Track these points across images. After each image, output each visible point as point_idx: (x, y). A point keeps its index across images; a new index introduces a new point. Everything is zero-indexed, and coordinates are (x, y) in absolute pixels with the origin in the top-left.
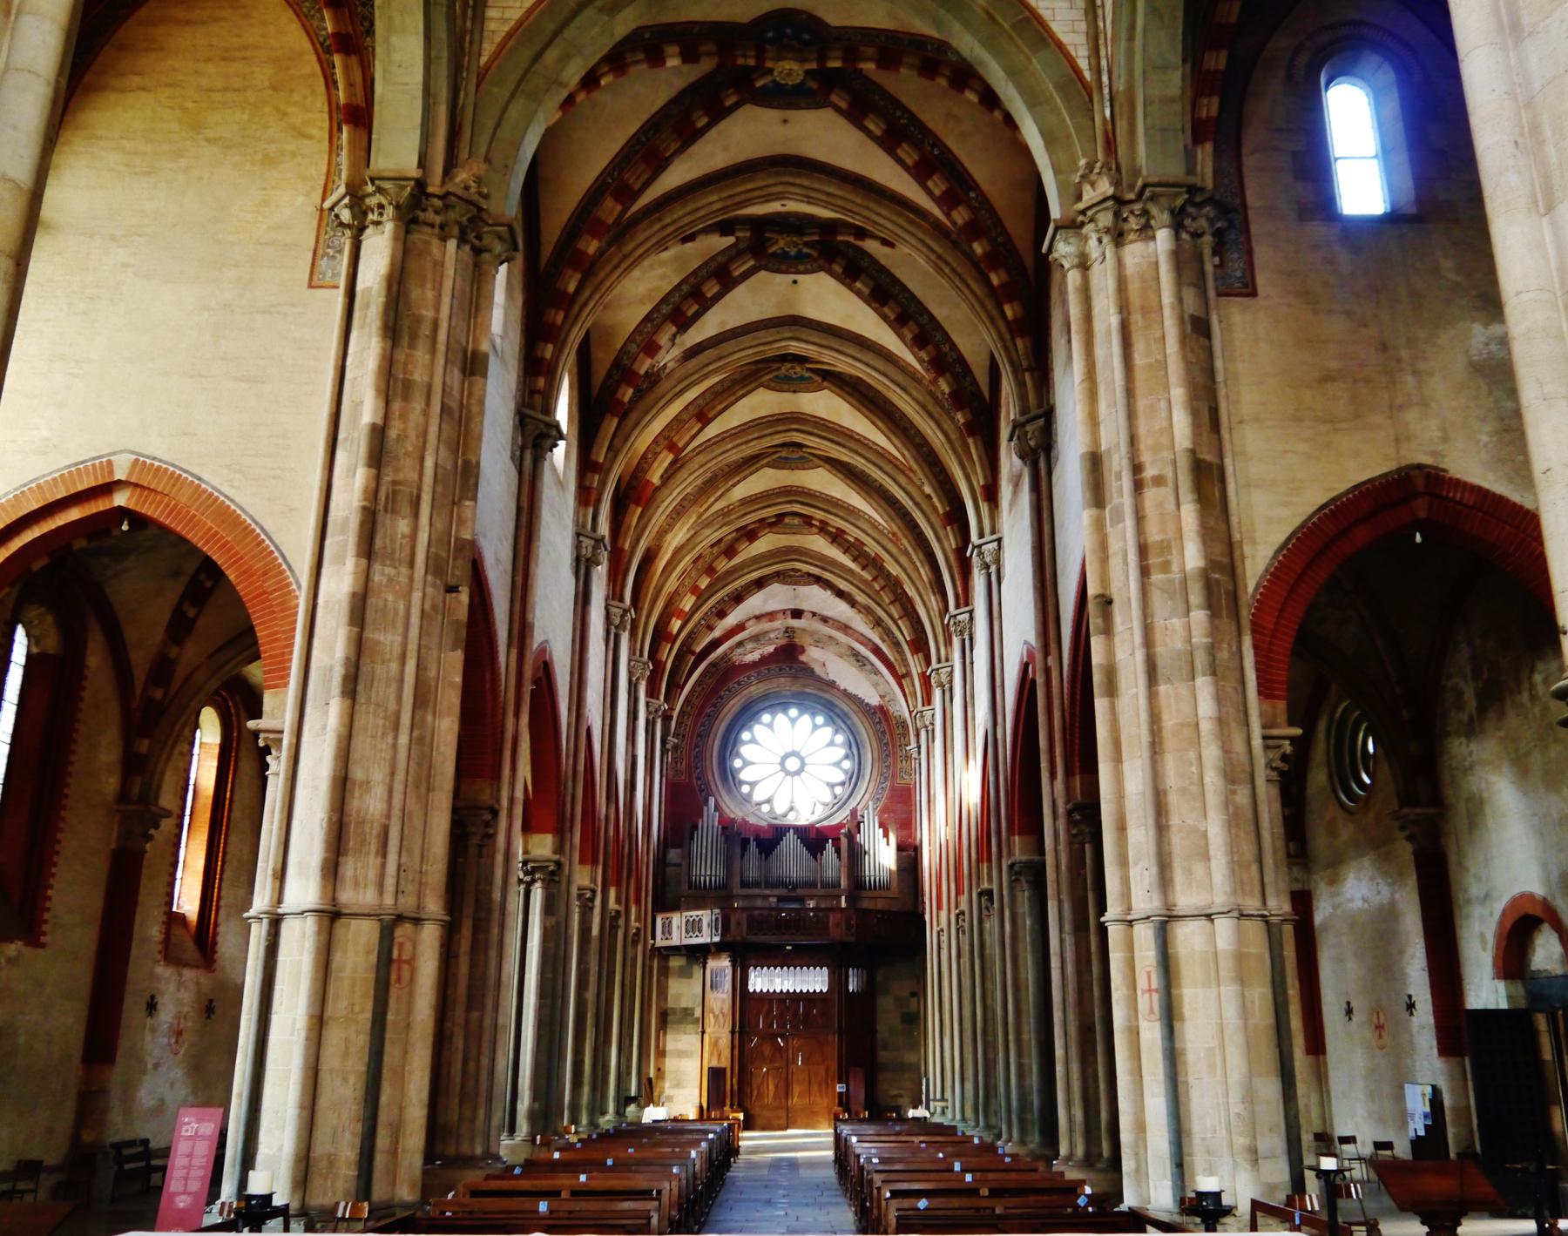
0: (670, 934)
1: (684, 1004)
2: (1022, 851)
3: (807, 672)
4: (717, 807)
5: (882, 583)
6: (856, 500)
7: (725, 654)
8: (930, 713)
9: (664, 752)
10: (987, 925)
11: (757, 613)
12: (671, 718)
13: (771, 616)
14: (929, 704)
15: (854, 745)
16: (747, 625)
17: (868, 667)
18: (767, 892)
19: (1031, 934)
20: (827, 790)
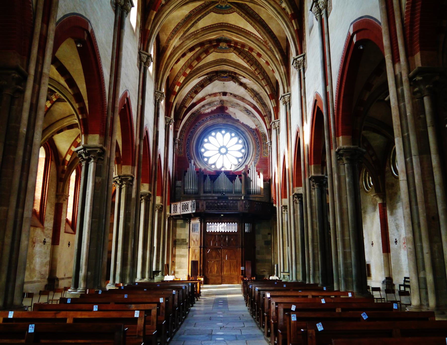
1: (182, 238)
2: (343, 144)
3: (229, 117)
4: (194, 164)
5: (259, 71)
6: (250, 28)
7: (198, 110)
8: (278, 122)
9: (174, 144)
10: (313, 193)
11: (210, 93)
12: (177, 131)
13: (215, 94)
15: (246, 144)
16: (206, 98)
17: (251, 115)
18: (214, 195)
19: (349, 186)
20: (236, 160)
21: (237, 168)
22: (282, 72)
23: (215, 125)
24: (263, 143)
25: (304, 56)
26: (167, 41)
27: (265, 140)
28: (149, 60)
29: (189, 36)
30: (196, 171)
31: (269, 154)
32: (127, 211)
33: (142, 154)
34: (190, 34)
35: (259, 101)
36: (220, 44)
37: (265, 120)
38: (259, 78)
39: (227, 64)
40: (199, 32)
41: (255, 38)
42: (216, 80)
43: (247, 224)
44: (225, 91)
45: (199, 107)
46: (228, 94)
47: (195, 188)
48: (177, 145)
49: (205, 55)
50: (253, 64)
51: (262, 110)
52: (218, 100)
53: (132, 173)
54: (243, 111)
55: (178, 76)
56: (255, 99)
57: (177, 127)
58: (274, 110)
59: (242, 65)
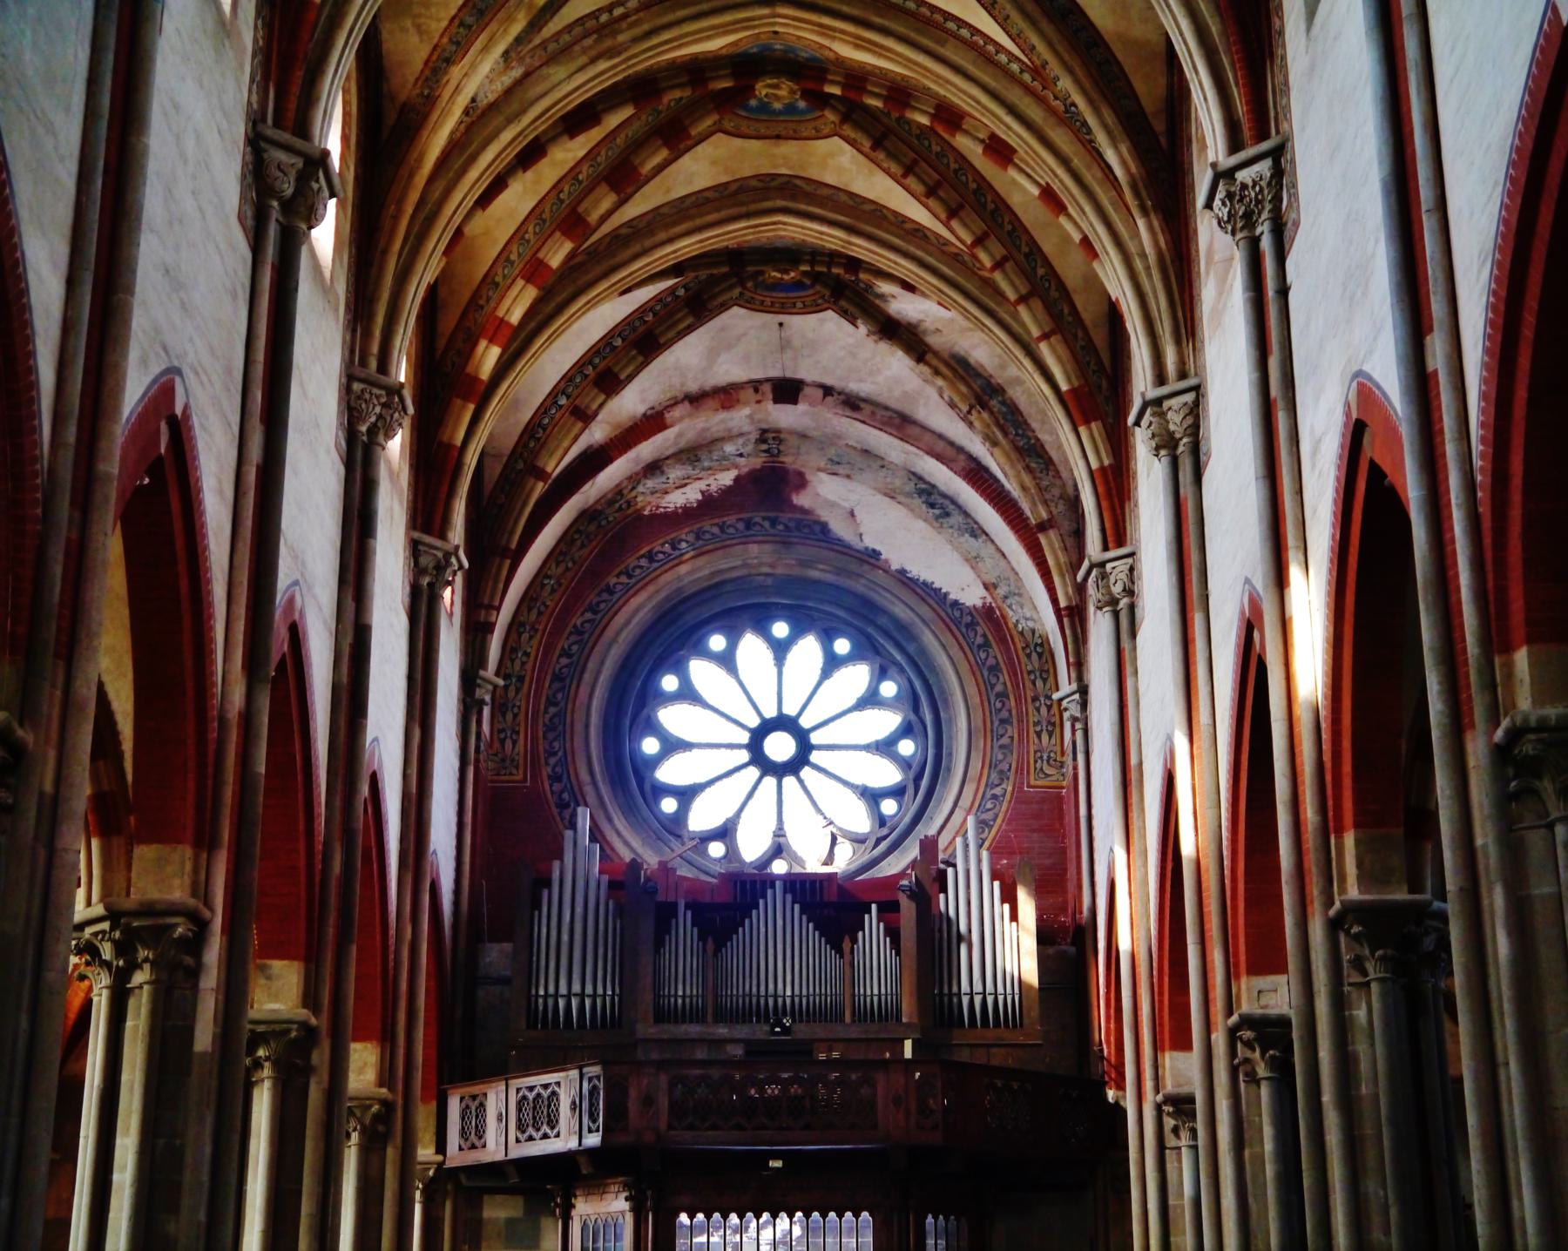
0: (480, 1134)
2: (1539, 699)
5: (1000, 251)
7: (618, 494)
8: (1122, 566)
10: (1361, 1014)
11: (693, 387)
12: (490, 628)
13: (726, 395)
14: (1121, 542)
16: (668, 416)
17: (957, 519)
18: (722, 1031)
21: (866, 858)
22: (1143, 255)
23: (729, 587)
24: (1030, 694)
25: (1279, 154)
26: (427, 73)
27: (1045, 681)
28: (315, 186)
29: (566, 38)
30: (605, 878)
31: (1075, 768)
32: (161, 1142)
33: (262, 769)
34: (569, 28)
35: (1006, 434)
36: (759, 86)
37: (1041, 550)
38: (1002, 295)
39: (803, 207)
40: (625, 16)
41: (972, 46)
42: (735, 309)
43: (936, 1218)
44: (789, 374)
45: (629, 473)
46: (807, 390)
47: (600, 991)
48: (486, 711)
49: (664, 154)
50: (961, 207)
51: (1024, 488)
52: (746, 428)
53: (194, 894)
55: (497, 285)
56: (977, 424)
57: (486, 601)
58: (1101, 490)
59: (895, 213)
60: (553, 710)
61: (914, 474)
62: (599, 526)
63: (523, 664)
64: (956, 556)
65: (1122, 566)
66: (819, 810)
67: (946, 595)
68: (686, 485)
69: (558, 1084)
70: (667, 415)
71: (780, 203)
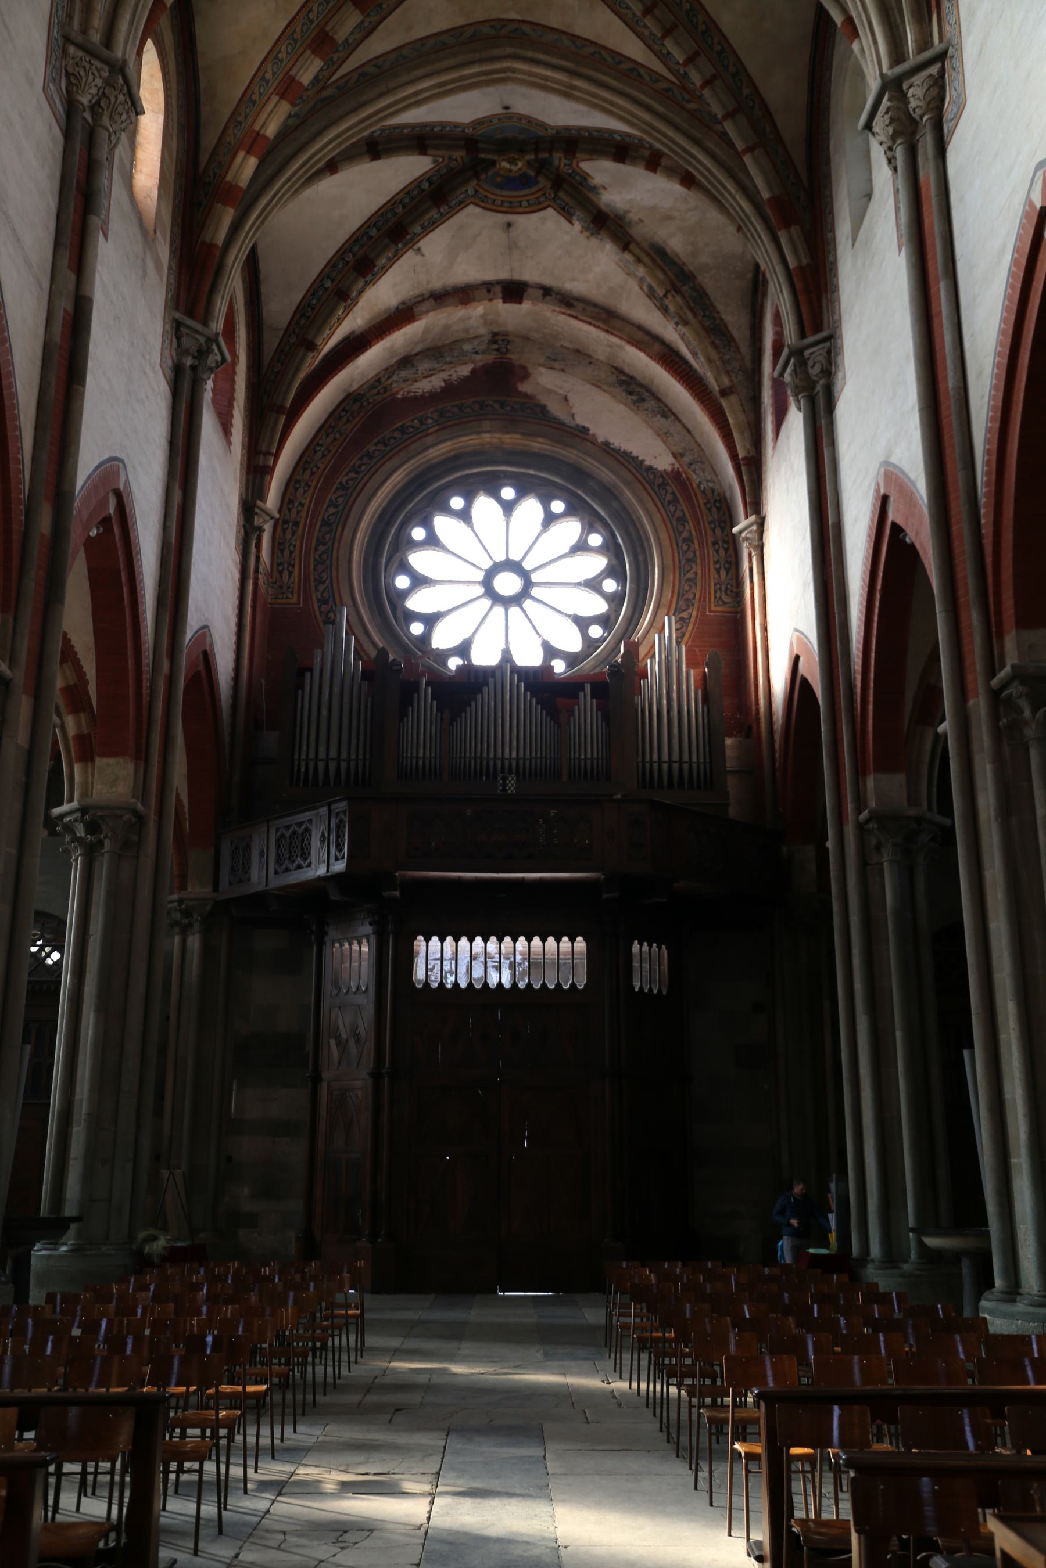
0: (246, 869)
7: (378, 383)
8: (819, 351)
11: (437, 284)
14: (818, 328)
20: (575, 631)
35: (695, 315)
39: (529, 54)
43: (641, 945)
44: (516, 277)
45: (385, 366)
46: (530, 291)
54: (605, 387)
55: (254, 103)
56: (672, 308)
57: (264, 448)
58: (799, 285)
60: (321, 548)
61: (616, 368)
62: (362, 406)
63: (298, 512)
64: (650, 431)
65: (819, 351)
66: (538, 634)
67: (642, 461)
68: (431, 375)
69: (310, 821)
70: (415, 310)
71: (509, 50)
